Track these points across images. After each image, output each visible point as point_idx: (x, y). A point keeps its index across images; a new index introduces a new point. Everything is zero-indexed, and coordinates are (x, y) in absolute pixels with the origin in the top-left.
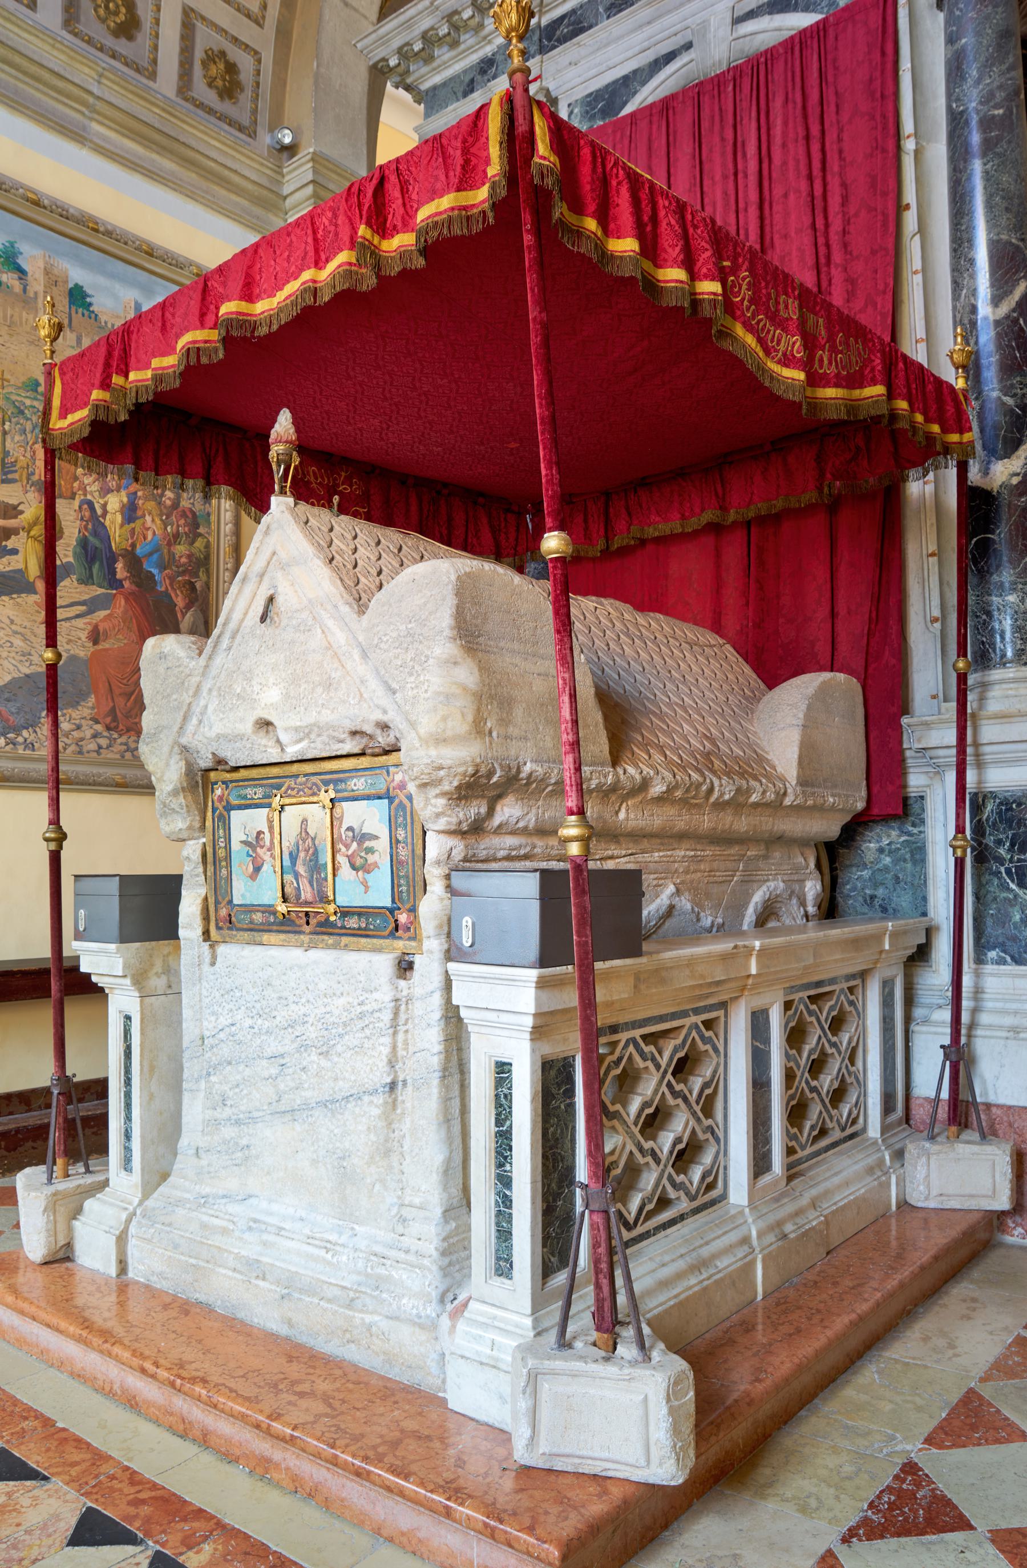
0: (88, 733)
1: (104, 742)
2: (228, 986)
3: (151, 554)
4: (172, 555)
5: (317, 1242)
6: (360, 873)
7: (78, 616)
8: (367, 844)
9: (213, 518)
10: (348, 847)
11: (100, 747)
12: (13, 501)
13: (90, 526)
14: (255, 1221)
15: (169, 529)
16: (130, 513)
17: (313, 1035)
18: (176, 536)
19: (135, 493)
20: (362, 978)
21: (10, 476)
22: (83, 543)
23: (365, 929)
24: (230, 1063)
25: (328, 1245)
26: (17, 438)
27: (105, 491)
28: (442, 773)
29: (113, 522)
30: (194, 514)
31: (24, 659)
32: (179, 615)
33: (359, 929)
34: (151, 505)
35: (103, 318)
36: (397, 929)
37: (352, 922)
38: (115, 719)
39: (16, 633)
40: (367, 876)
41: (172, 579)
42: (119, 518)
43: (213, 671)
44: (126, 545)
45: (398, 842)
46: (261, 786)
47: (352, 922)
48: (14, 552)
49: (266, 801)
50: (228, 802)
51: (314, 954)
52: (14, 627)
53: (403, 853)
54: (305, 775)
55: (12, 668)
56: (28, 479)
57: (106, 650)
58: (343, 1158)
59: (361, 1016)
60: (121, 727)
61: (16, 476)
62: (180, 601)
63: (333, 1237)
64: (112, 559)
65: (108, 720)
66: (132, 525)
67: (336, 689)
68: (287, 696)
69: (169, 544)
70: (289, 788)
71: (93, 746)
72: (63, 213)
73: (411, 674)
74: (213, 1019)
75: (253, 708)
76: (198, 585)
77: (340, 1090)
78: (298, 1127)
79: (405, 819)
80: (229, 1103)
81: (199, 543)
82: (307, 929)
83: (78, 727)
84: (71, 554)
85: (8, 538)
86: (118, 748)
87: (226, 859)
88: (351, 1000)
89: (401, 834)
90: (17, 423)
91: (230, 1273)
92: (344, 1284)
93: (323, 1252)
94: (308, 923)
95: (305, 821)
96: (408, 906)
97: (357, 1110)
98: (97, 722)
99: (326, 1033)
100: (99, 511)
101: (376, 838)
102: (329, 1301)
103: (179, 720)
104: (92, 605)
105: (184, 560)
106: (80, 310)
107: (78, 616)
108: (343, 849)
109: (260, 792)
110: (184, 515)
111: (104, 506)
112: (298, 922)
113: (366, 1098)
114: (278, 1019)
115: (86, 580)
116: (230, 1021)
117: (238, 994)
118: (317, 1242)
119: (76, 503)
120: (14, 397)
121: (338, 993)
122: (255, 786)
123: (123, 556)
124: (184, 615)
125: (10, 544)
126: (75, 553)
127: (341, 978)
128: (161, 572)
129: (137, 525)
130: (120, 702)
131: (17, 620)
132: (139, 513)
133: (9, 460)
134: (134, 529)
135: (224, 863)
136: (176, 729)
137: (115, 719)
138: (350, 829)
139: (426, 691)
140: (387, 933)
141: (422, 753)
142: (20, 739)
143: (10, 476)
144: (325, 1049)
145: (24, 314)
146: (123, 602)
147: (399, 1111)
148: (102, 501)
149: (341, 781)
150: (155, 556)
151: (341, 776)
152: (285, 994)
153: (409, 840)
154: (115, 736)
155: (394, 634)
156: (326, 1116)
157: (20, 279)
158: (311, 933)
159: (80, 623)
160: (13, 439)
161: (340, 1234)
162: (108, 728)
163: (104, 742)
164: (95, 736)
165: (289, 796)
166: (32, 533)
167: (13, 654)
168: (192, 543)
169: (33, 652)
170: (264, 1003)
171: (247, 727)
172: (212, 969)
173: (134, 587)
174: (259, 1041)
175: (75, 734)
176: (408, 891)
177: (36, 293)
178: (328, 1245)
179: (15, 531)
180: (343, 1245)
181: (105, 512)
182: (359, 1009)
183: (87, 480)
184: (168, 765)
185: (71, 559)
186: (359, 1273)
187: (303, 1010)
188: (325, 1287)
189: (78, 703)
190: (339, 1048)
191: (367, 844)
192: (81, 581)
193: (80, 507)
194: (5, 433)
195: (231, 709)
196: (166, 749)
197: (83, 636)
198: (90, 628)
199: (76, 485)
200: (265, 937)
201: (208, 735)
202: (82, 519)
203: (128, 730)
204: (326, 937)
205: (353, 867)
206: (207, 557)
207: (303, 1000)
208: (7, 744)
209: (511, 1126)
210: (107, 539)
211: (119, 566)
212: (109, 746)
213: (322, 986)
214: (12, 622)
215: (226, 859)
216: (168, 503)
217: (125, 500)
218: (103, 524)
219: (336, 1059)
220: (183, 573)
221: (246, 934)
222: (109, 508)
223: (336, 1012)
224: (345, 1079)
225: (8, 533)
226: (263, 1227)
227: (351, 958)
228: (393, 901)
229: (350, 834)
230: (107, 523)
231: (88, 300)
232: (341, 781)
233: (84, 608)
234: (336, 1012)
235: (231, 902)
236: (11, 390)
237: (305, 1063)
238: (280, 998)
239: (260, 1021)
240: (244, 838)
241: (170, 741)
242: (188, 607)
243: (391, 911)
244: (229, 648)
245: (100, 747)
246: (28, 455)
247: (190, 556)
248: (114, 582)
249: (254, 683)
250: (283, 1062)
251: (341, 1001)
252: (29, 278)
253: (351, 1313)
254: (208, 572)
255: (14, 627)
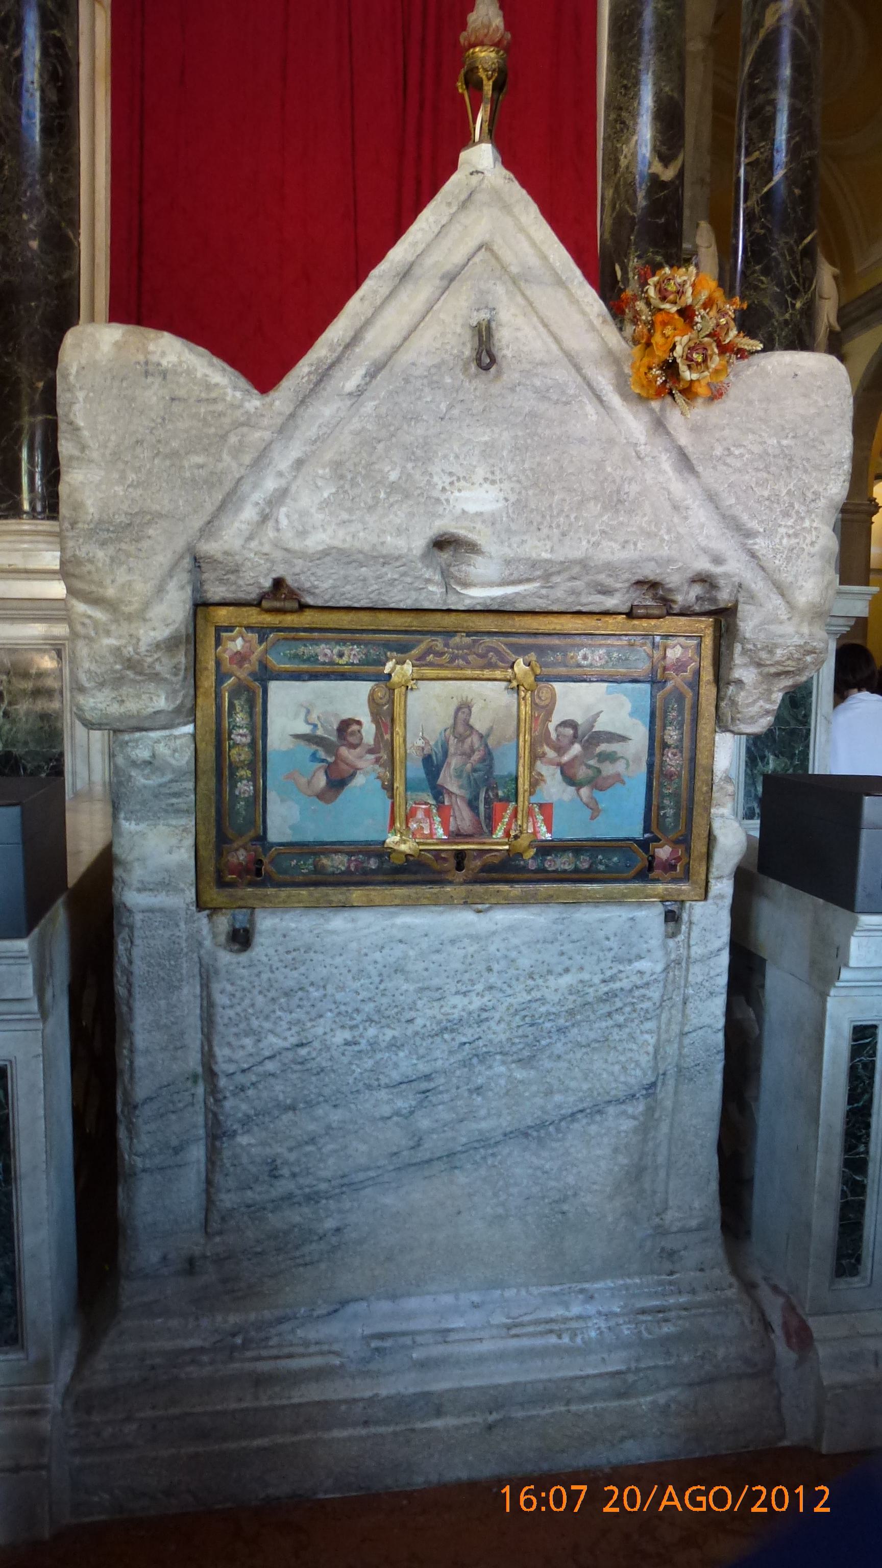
2: (291, 983)
5: (531, 1329)
6: (584, 791)
8: (603, 747)
10: (560, 750)
14: (382, 1336)
17: (503, 1037)
20: (613, 943)
23: (588, 871)
24: (293, 1108)
25: (555, 1327)
28: (809, 659)
33: (576, 870)
36: (650, 868)
37: (564, 862)
40: (598, 794)
43: (308, 429)
45: (665, 746)
46: (358, 643)
47: (564, 862)
49: (372, 669)
50: (263, 666)
51: (502, 917)
53: (673, 761)
54: (469, 634)
58: (565, 1199)
59: (609, 996)
63: (558, 1312)
67: (630, 512)
68: (520, 505)
70: (429, 651)
73: (786, 514)
74: (248, 1042)
75: (435, 515)
77: (559, 1107)
78: (461, 1178)
79: (681, 711)
80: (285, 1171)
82: (460, 876)
87: (252, 766)
88: (586, 976)
89: (672, 735)
91: (364, 1432)
92: (610, 1369)
93: (553, 1340)
94: (460, 867)
95: (464, 708)
96: (672, 836)
97: (593, 1129)
99: (529, 1030)
101: (623, 739)
102: (584, 1399)
103: (209, 508)
108: (551, 754)
109: (352, 654)
112: (436, 866)
113: (611, 1110)
114: (419, 1022)
116: (294, 1040)
117: (315, 994)
118: (531, 1329)
121: (560, 969)
122: (343, 642)
127: (568, 947)
135: (244, 773)
136: (197, 522)
138: (564, 724)
139: (813, 544)
140: (632, 873)
141: (789, 628)
144: (526, 1053)
147: (657, 1115)
149: (553, 649)
151: (556, 641)
152: (436, 982)
153: (686, 743)
155: (757, 449)
156: (525, 1149)
158: (466, 882)
161: (566, 1305)
165: (431, 665)
170: (385, 1001)
171: (419, 543)
172: (243, 958)
174: (369, 1063)
176: (677, 815)
178: (555, 1327)
180: (579, 1318)
182: (605, 988)
184: (160, 590)
186: (627, 1345)
187: (477, 1003)
188: (577, 1385)
190: (559, 1048)
191: (603, 747)
195: (371, 509)
196: (163, 559)
200: (357, 894)
201: (295, 544)
204: (505, 888)
205: (570, 779)
207: (479, 987)
209: (871, 1100)
213: (525, 962)
215: (252, 766)
219: (548, 1064)
221: (304, 892)
223: (553, 997)
224: (567, 1090)
226: (408, 1341)
227: (587, 915)
228: (647, 829)
229: (570, 732)
232: (553, 649)
234: (553, 997)
235: (262, 838)
237: (480, 1081)
238: (422, 989)
239: (372, 1031)
240: (305, 729)
241: (180, 544)
243: (644, 845)
244: (359, 393)
249: (435, 469)
250: (424, 1085)
251: (566, 980)
253: (633, 1402)
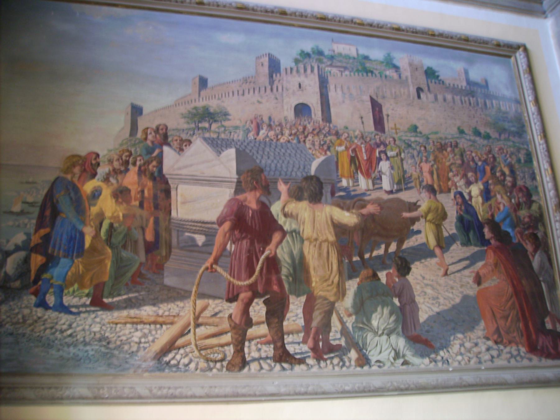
0: (483, 348)
1: (495, 353)
3: (504, 219)
4: (518, 218)
7: (465, 268)
9: (540, 189)
11: (492, 357)
12: (413, 200)
13: (463, 208)
15: (513, 201)
16: (487, 194)
18: (518, 206)
19: (487, 182)
21: (409, 185)
22: (461, 219)
26: (410, 161)
27: (469, 183)
29: (477, 203)
30: (527, 189)
31: (434, 302)
32: (531, 257)
34: (498, 188)
35: (447, 82)
38: (500, 335)
39: (427, 285)
41: (521, 234)
42: (480, 199)
44: (488, 216)
48: (419, 232)
52: (425, 281)
55: (427, 309)
56: (420, 186)
57: (487, 288)
60: (505, 341)
61: (413, 184)
62: (529, 248)
64: (480, 227)
65: (495, 337)
66: (489, 203)
69: (515, 211)
71: (487, 357)
72: (415, 32)
76: (540, 235)
81: (534, 207)
83: (476, 345)
84: (454, 228)
85: (413, 223)
86: (505, 356)
90: (408, 153)
98: (488, 339)
100: (467, 197)
104: (473, 259)
105: (527, 220)
106: (433, 81)
107: (465, 268)
110: (520, 190)
111: (470, 193)
115: (467, 243)
119: (452, 195)
120: (404, 138)
123: (487, 224)
124: (533, 256)
125: (415, 227)
126: (456, 227)
128: (513, 230)
129: (492, 202)
130: (501, 323)
131: (427, 277)
132: (492, 194)
133: (407, 175)
134: (490, 205)
137: (500, 335)
142: (439, 358)
143: (409, 185)
145: (402, 90)
146: (492, 254)
148: (467, 191)
150: (508, 221)
154: (502, 347)
157: (396, 71)
159: (467, 272)
160: (407, 162)
162: (496, 343)
163: (495, 353)
164: (488, 349)
166: (428, 218)
167: (427, 300)
168: (530, 207)
169: (440, 296)
173: (498, 243)
175: (475, 350)
177: (407, 77)
179: (417, 219)
181: (471, 197)
183: (456, 179)
185: (454, 231)
189: (473, 328)
192: (464, 244)
193: (455, 197)
194: (402, 160)
197: (471, 280)
198: (474, 275)
199: (450, 183)
202: (457, 204)
203: (510, 342)
206: (541, 215)
208: (431, 362)
210: (474, 214)
211: (486, 230)
212: (499, 356)
214: (424, 278)
216: (509, 184)
217: (482, 187)
218: (471, 206)
220: (528, 228)
222: (473, 194)
225: (414, 220)
230: (473, 204)
231: (437, 74)
233: (467, 262)
236: (401, 134)
242: (535, 251)
245: (492, 357)
246: (418, 170)
247: (530, 217)
248: (484, 242)
252: (401, 70)
254: (544, 225)
255: (425, 281)
